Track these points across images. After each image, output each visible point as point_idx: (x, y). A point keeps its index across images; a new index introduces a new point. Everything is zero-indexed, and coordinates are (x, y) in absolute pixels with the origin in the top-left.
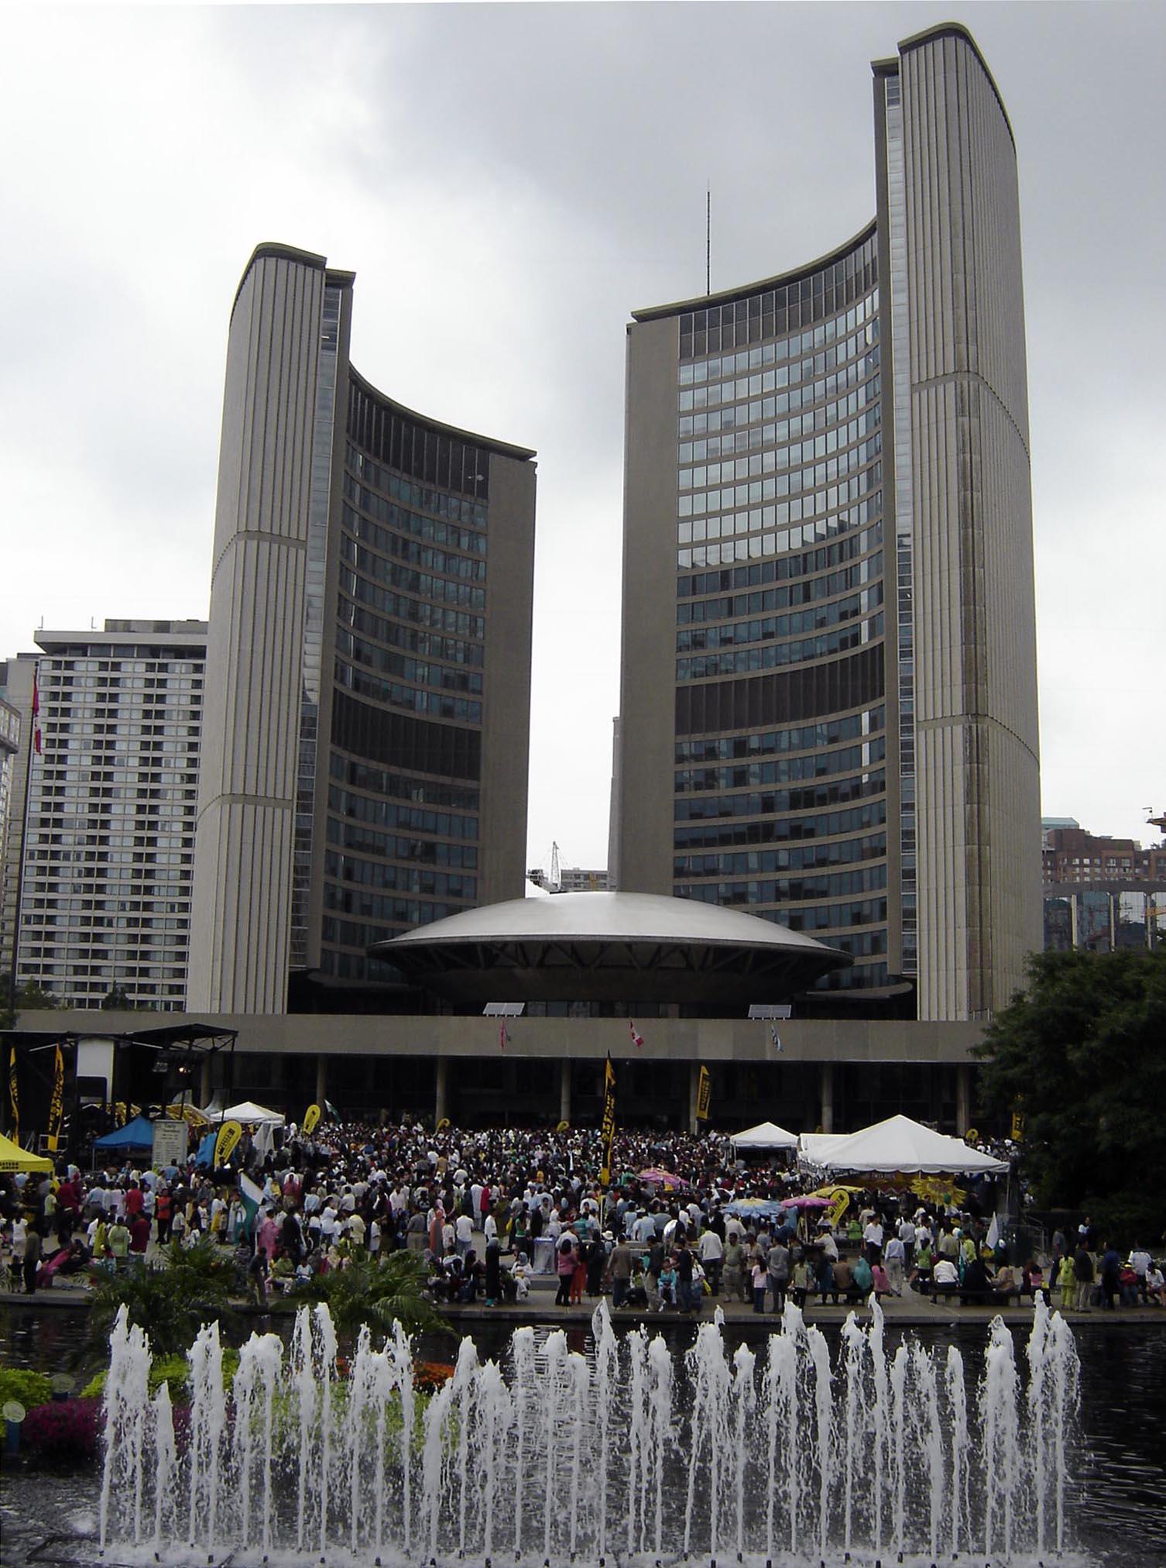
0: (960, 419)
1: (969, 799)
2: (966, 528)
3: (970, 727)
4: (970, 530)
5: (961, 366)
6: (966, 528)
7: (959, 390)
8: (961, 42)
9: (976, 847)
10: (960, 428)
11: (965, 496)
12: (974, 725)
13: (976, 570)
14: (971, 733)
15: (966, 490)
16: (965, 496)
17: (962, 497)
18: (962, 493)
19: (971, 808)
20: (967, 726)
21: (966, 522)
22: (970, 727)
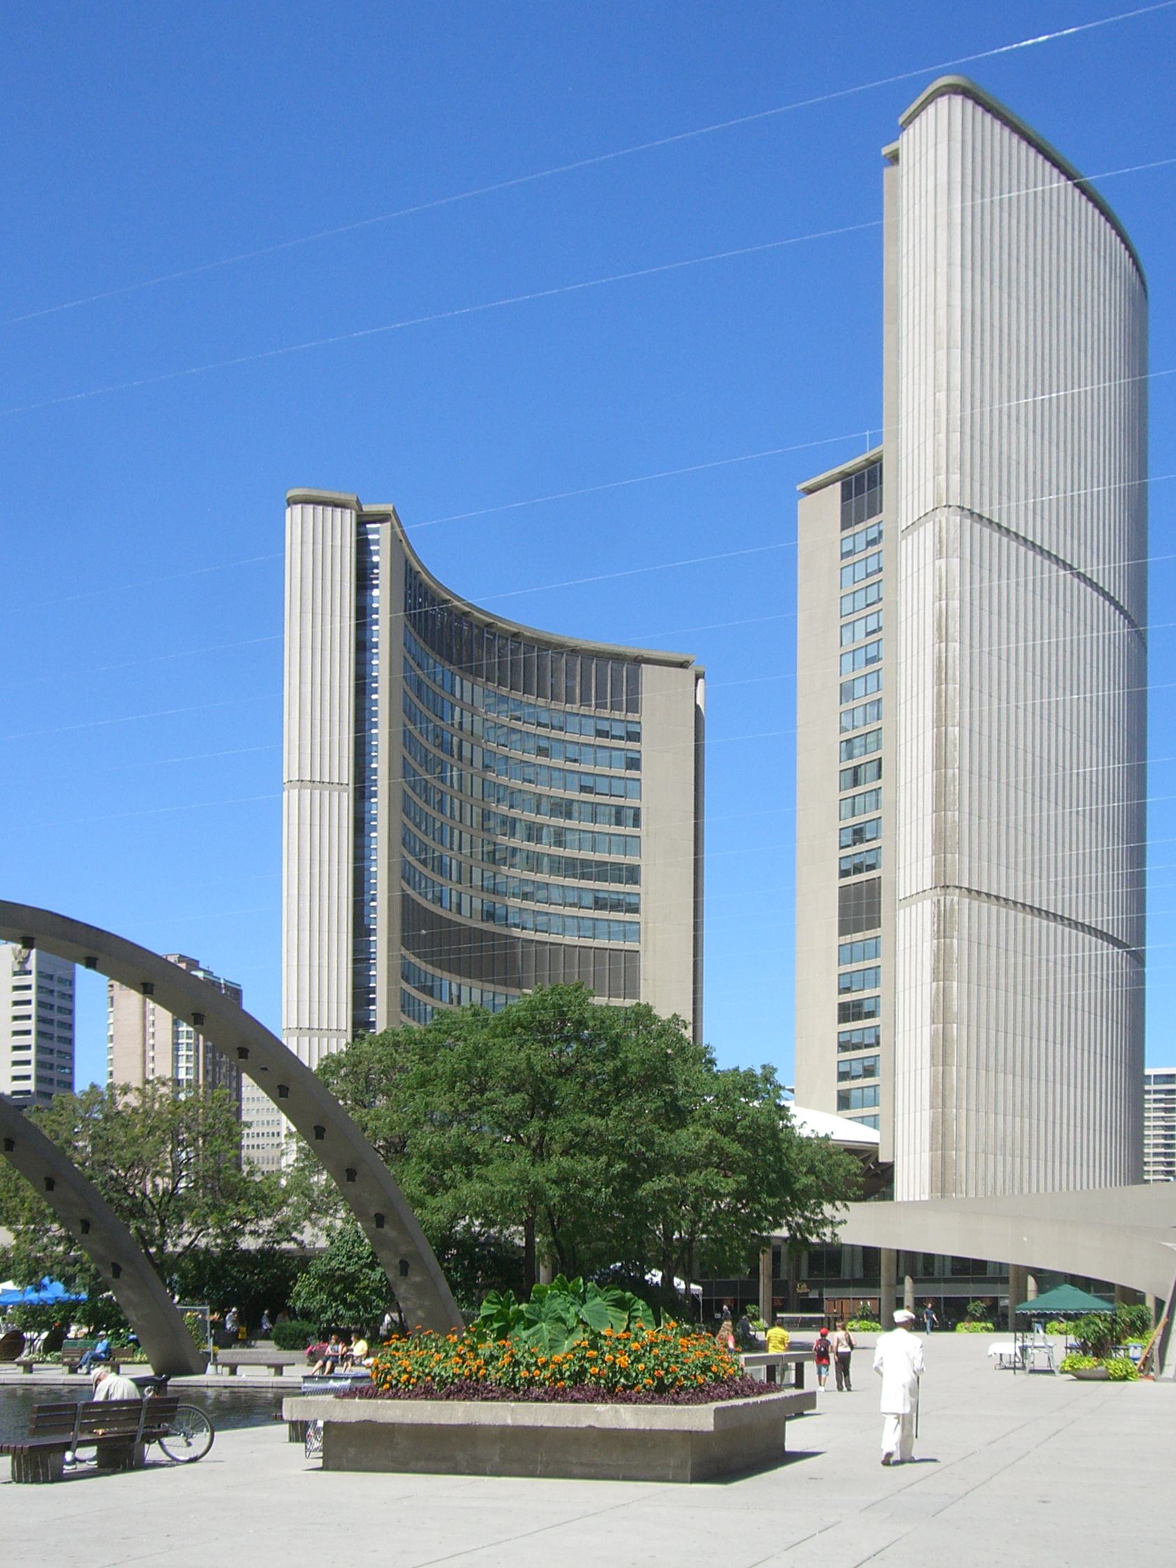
0: (937, 561)
1: (935, 979)
2: (940, 684)
3: (939, 901)
4: (943, 686)
5: (940, 501)
6: (940, 684)
7: (937, 529)
8: (958, 100)
9: (941, 1025)
10: (937, 573)
11: (940, 648)
12: (942, 898)
13: (950, 729)
14: (939, 907)
15: (941, 642)
16: (940, 648)
17: (936, 650)
18: (937, 646)
19: (938, 988)
20: (935, 899)
21: (939, 678)
22: (939, 901)
